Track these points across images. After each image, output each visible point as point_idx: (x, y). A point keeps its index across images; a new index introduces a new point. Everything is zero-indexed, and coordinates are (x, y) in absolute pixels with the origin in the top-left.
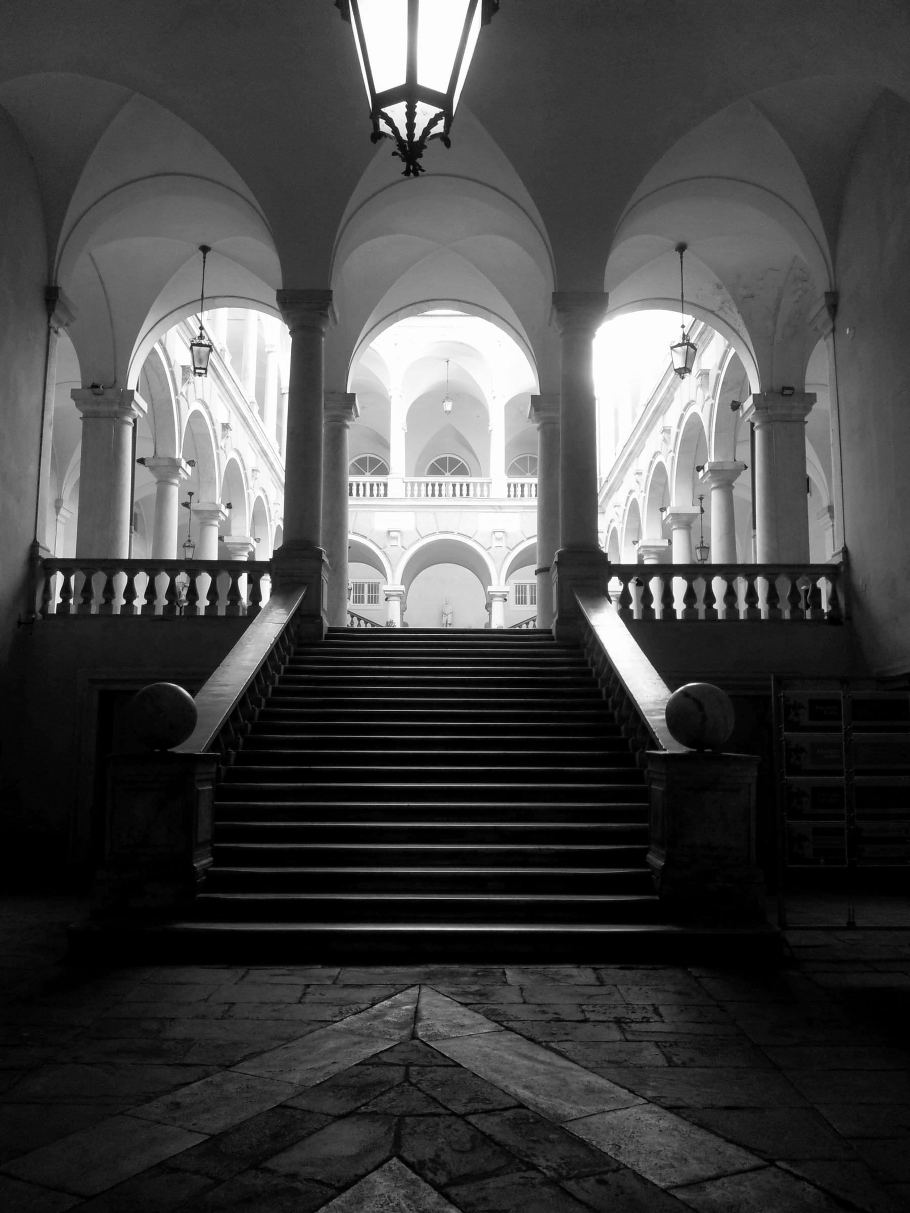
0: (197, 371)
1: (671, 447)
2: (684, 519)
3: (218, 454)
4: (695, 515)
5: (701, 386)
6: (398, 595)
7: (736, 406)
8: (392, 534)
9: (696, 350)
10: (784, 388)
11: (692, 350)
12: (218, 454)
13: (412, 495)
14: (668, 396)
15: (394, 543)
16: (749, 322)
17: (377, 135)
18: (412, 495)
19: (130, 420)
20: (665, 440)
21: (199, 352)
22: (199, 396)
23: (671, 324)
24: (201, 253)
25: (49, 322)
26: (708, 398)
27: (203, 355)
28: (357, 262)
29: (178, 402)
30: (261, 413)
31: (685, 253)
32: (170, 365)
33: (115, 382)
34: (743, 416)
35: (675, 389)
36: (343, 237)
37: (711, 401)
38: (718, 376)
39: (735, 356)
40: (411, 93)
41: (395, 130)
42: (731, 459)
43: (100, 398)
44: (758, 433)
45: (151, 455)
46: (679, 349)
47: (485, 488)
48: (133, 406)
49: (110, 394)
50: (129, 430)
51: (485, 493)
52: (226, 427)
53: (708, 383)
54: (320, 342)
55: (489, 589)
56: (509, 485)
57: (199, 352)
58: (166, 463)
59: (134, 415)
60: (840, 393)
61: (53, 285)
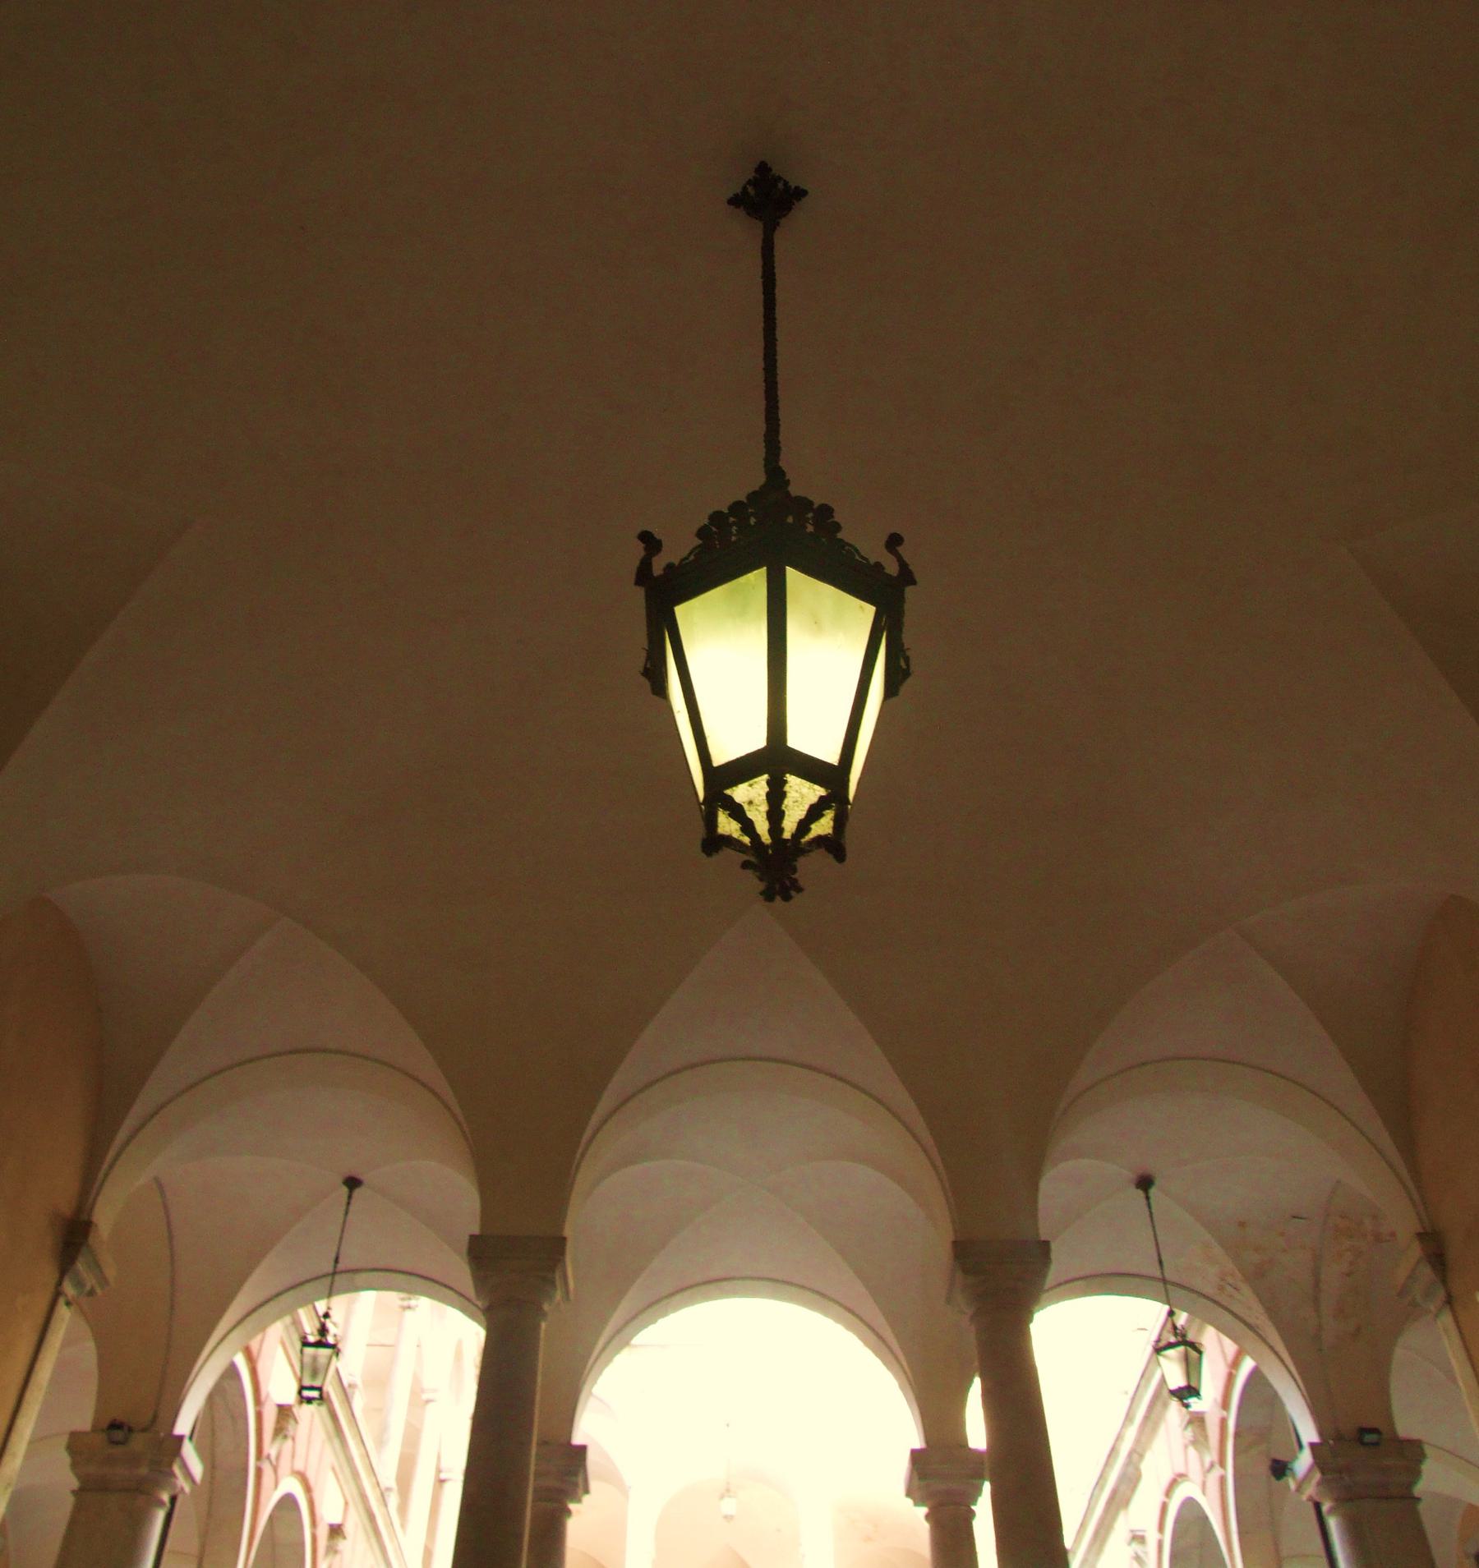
0: (306, 1393)
5: (1194, 1442)
7: (1280, 1469)
9: (1200, 1352)
10: (1364, 1431)
11: (1193, 1354)
14: (1131, 1469)
16: (1272, 1312)
17: (715, 842)
19: (165, 1497)
21: (315, 1358)
22: (299, 1466)
23: (1144, 1315)
24: (345, 1190)
25: (60, 1283)
26: (1212, 1465)
27: (322, 1361)
30: (403, 1509)
31: (1153, 1191)
32: (258, 1401)
34: (1299, 1489)
35: (1141, 1456)
37: (1217, 1472)
38: (1223, 1422)
39: (1255, 1376)
40: (776, 760)
41: (748, 826)
43: (119, 1450)
46: (1171, 1352)
48: (176, 1469)
49: (138, 1442)
52: (336, 1531)
53: (1206, 1437)
54: (537, 1328)
57: (315, 1358)
59: (174, 1486)
61: (84, 1217)
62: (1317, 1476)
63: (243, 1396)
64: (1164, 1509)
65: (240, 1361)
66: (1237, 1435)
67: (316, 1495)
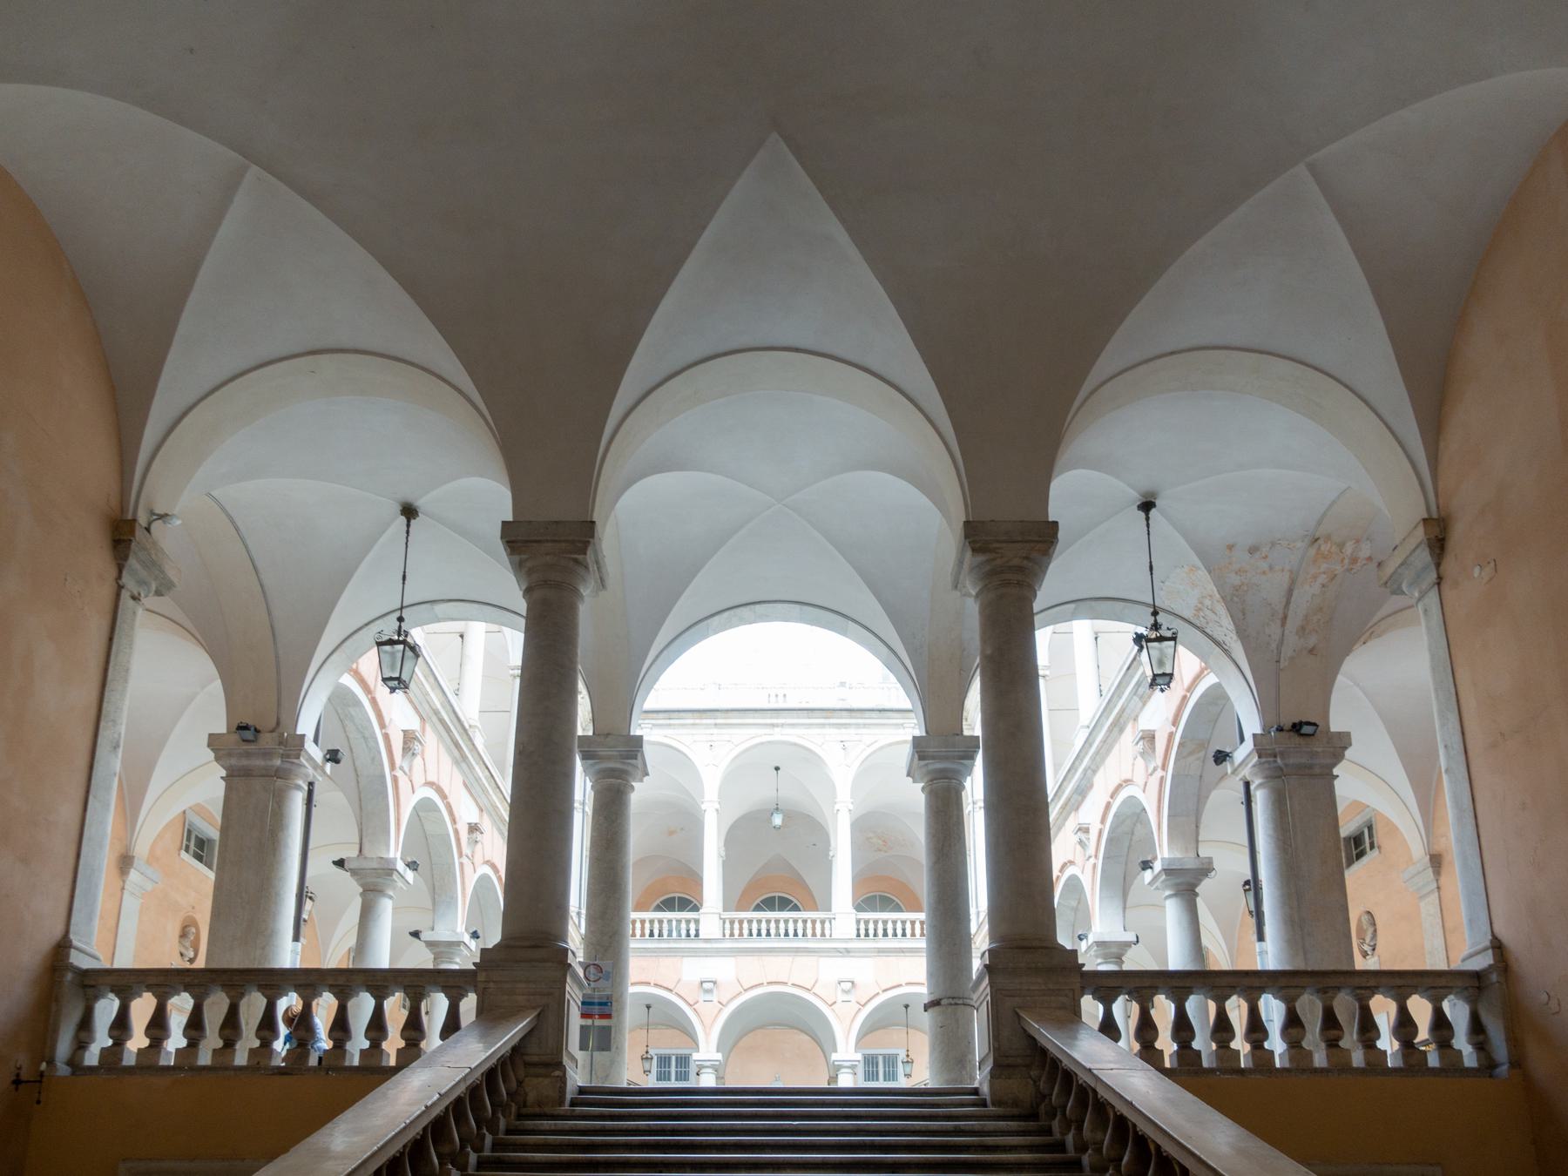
1: (1091, 850)
2: (1114, 950)
3: (461, 865)
4: (1128, 945)
5: (1142, 754)
6: (712, 1067)
8: (706, 986)
10: (1301, 724)
12: (461, 865)
13: (732, 934)
15: (708, 997)
18: (732, 934)
20: (1081, 842)
26: (1155, 769)
28: (642, 507)
29: (395, 779)
33: (278, 723)
35: (1095, 772)
36: (612, 449)
37: (1159, 773)
38: (1171, 736)
42: (1193, 855)
44: (1260, 798)
45: (354, 853)
47: (827, 925)
49: (267, 740)
50: (298, 801)
51: (827, 932)
52: (473, 828)
53: (1154, 749)
55: (834, 1057)
56: (858, 922)
58: (375, 865)
59: (307, 775)
60: (1463, 676)
62: (1256, 759)
63: (369, 720)
64: (1108, 806)
65: (347, 680)
66: (1181, 745)
67: (451, 800)
